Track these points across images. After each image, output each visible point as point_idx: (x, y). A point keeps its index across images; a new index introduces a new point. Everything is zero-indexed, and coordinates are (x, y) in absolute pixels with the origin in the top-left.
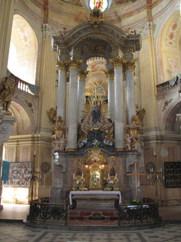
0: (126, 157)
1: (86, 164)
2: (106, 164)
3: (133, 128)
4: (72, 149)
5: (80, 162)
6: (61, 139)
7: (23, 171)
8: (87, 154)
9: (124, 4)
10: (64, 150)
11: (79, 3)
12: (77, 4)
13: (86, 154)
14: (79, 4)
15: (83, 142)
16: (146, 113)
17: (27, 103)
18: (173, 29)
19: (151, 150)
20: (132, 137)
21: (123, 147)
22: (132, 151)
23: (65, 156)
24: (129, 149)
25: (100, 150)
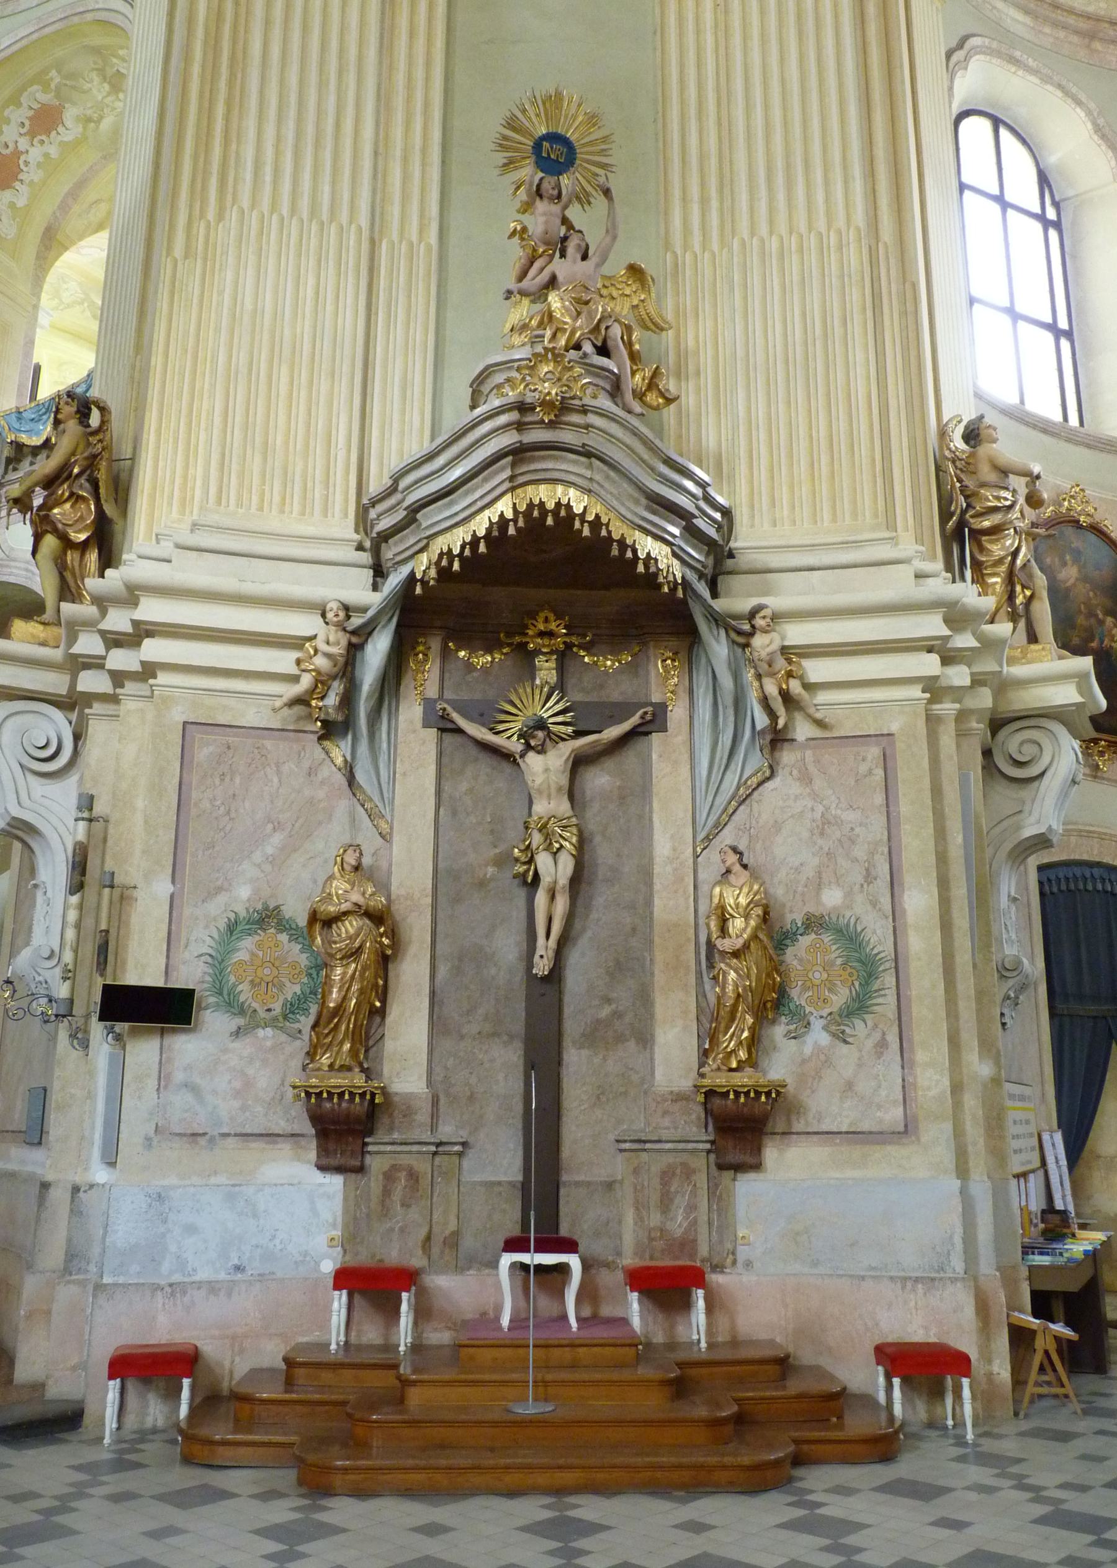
18: (32, 134)
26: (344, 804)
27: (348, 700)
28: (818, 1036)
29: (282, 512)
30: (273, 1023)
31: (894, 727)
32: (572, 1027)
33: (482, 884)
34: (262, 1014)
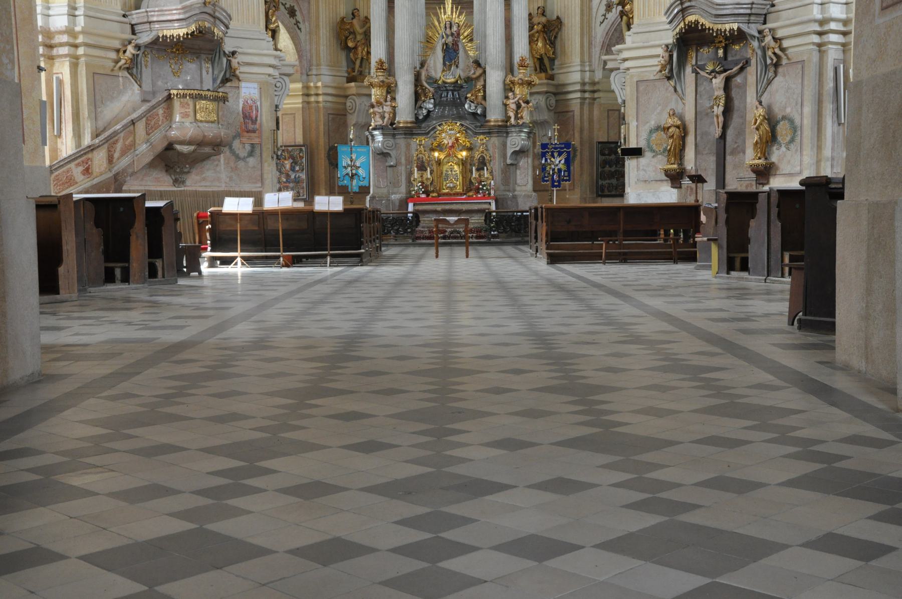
0: (507, 137)
1: (433, 150)
2: (470, 149)
3: (520, 82)
4: (407, 123)
5: (422, 147)
6: (384, 103)
7: (288, 166)
8: (435, 132)
10: (392, 124)
13: (432, 132)
15: (425, 109)
16: (563, 28)
17: (285, 8)
19: (572, 113)
20: (519, 99)
21: (504, 118)
22: (518, 125)
23: (394, 136)
24: (512, 120)
25: (458, 124)
26: (675, 96)
27: (671, 70)
28: (783, 149)
29: (659, 15)
30: (661, 154)
31: (805, 58)
32: (728, 150)
33: (707, 114)
34: (658, 152)
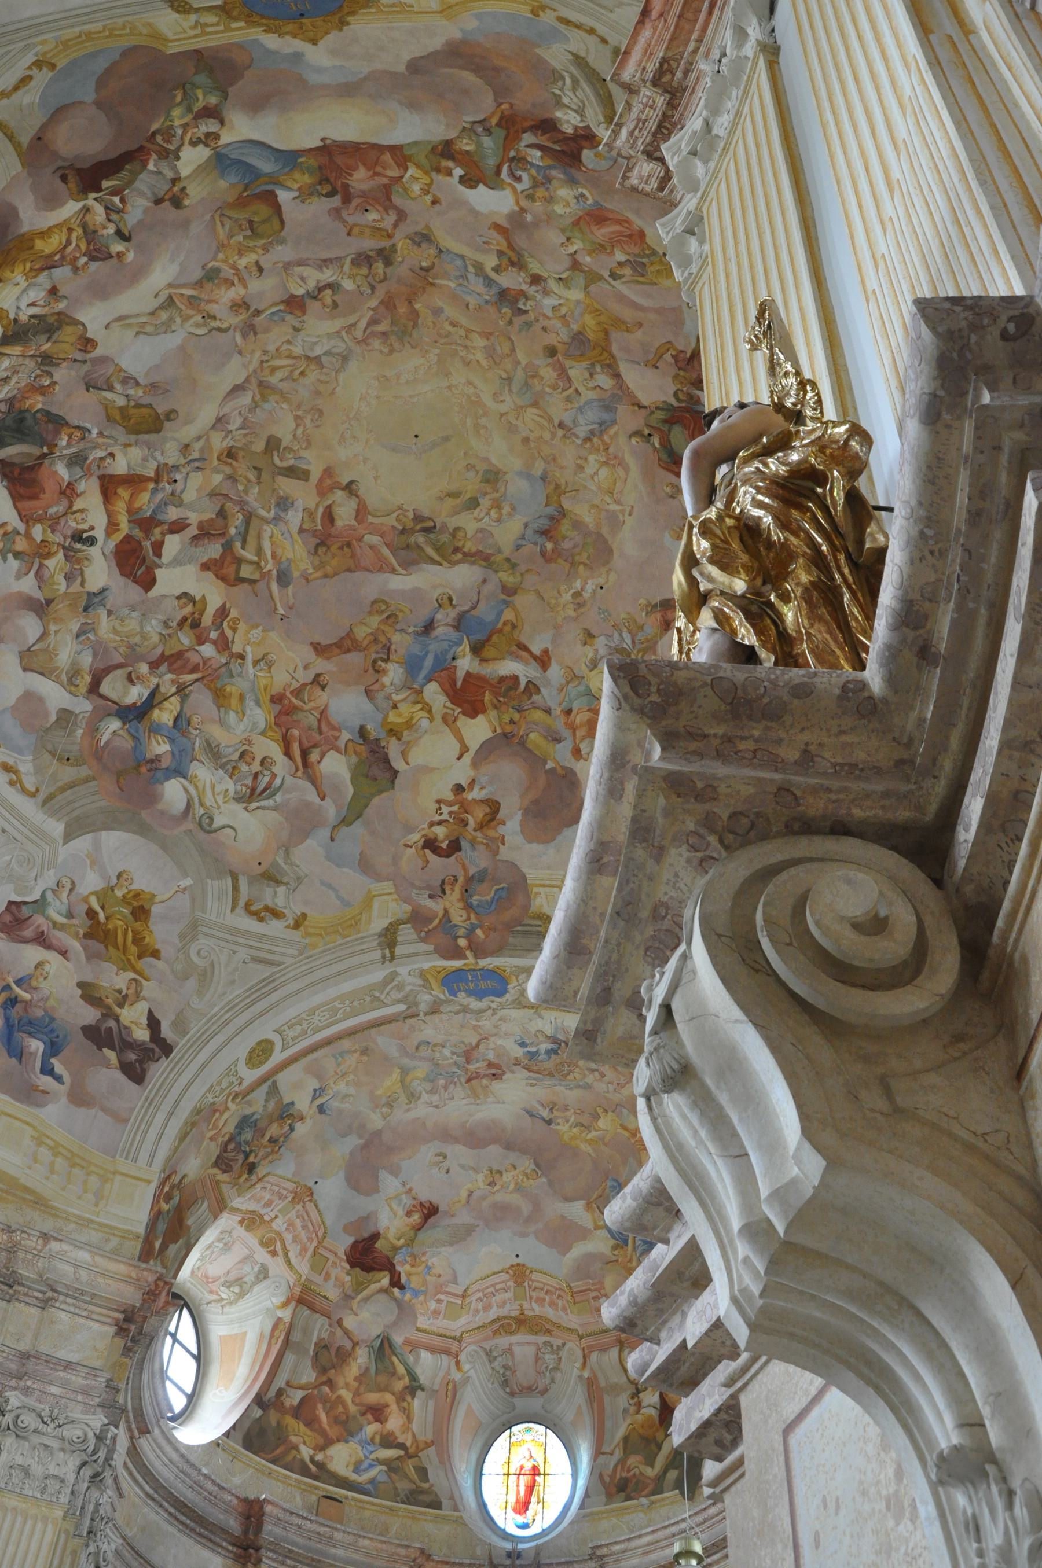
9: (644, 1501)
11: (425, 1485)
12: (413, 1492)
14: (423, 1492)
